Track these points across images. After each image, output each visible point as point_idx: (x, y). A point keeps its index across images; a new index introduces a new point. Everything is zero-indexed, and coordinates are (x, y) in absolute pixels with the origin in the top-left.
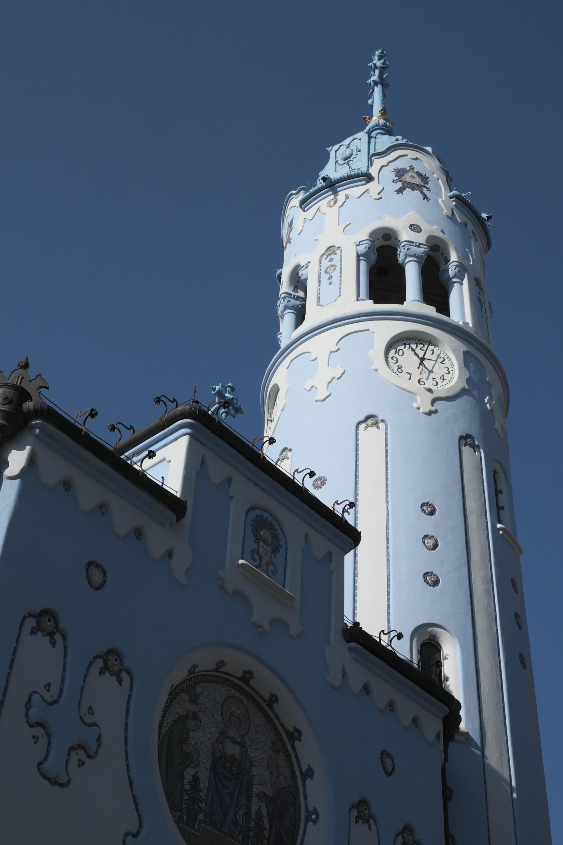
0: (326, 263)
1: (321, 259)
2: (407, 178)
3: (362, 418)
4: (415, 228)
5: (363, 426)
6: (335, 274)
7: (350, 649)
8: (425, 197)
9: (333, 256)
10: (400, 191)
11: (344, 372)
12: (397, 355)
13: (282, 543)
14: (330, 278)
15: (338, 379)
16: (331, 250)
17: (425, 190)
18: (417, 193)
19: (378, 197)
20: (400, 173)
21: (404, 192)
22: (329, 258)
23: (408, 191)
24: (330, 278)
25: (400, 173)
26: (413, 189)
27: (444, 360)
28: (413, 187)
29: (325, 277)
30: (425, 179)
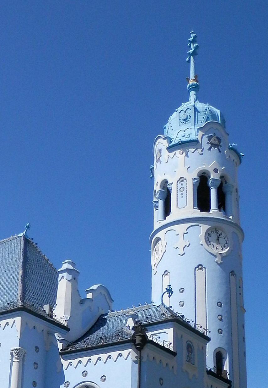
0: (180, 186)
1: (177, 182)
3: (197, 266)
4: (216, 170)
5: (197, 269)
6: (184, 192)
7: (208, 376)
9: (182, 182)
10: (210, 149)
11: (190, 244)
12: (209, 237)
13: (193, 350)
14: (182, 194)
15: (188, 247)
16: (182, 179)
19: (201, 153)
22: (181, 183)
24: (182, 194)
27: (225, 237)
29: (180, 193)
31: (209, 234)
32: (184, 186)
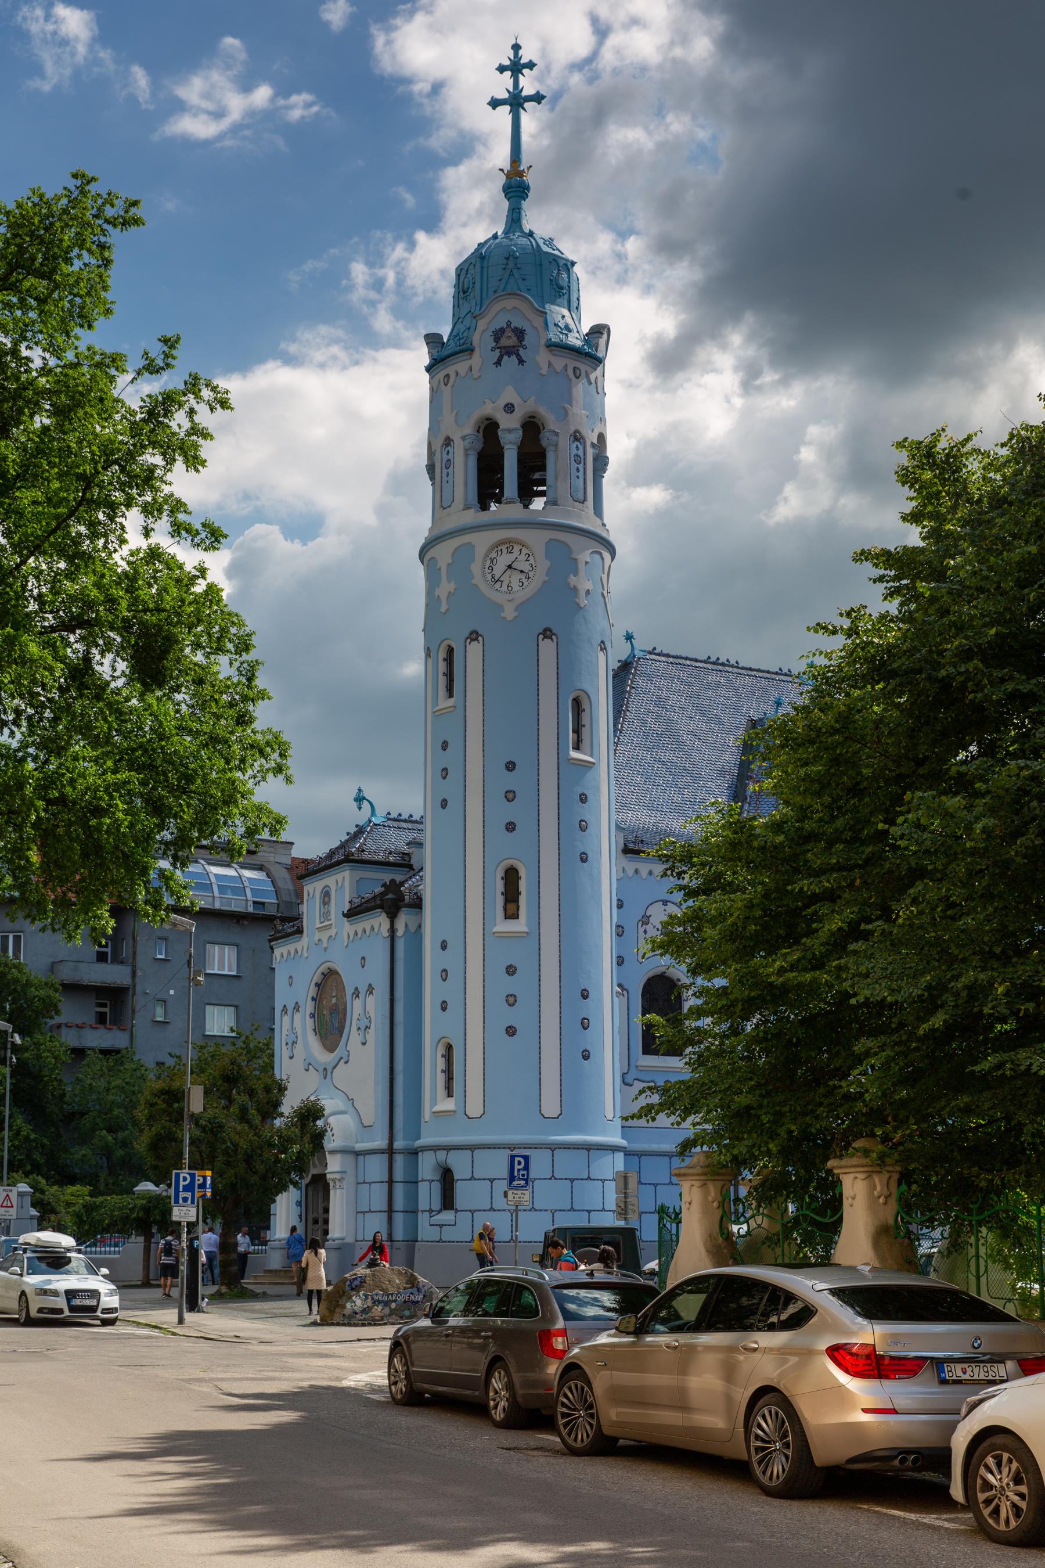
0: (445, 457)
2: (504, 342)
3: (467, 635)
6: (450, 470)
8: (521, 362)
9: (449, 448)
10: (498, 363)
16: (448, 442)
17: (521, 351)
18: (514, 357)
20: (498, 335)
21: (502, 363)
23: (505, 358)
25: (498, 335)
26: (509, 354)
28: (508, 351)
30: (520, 334)
31: (492, 562)
32: (450, 456)
